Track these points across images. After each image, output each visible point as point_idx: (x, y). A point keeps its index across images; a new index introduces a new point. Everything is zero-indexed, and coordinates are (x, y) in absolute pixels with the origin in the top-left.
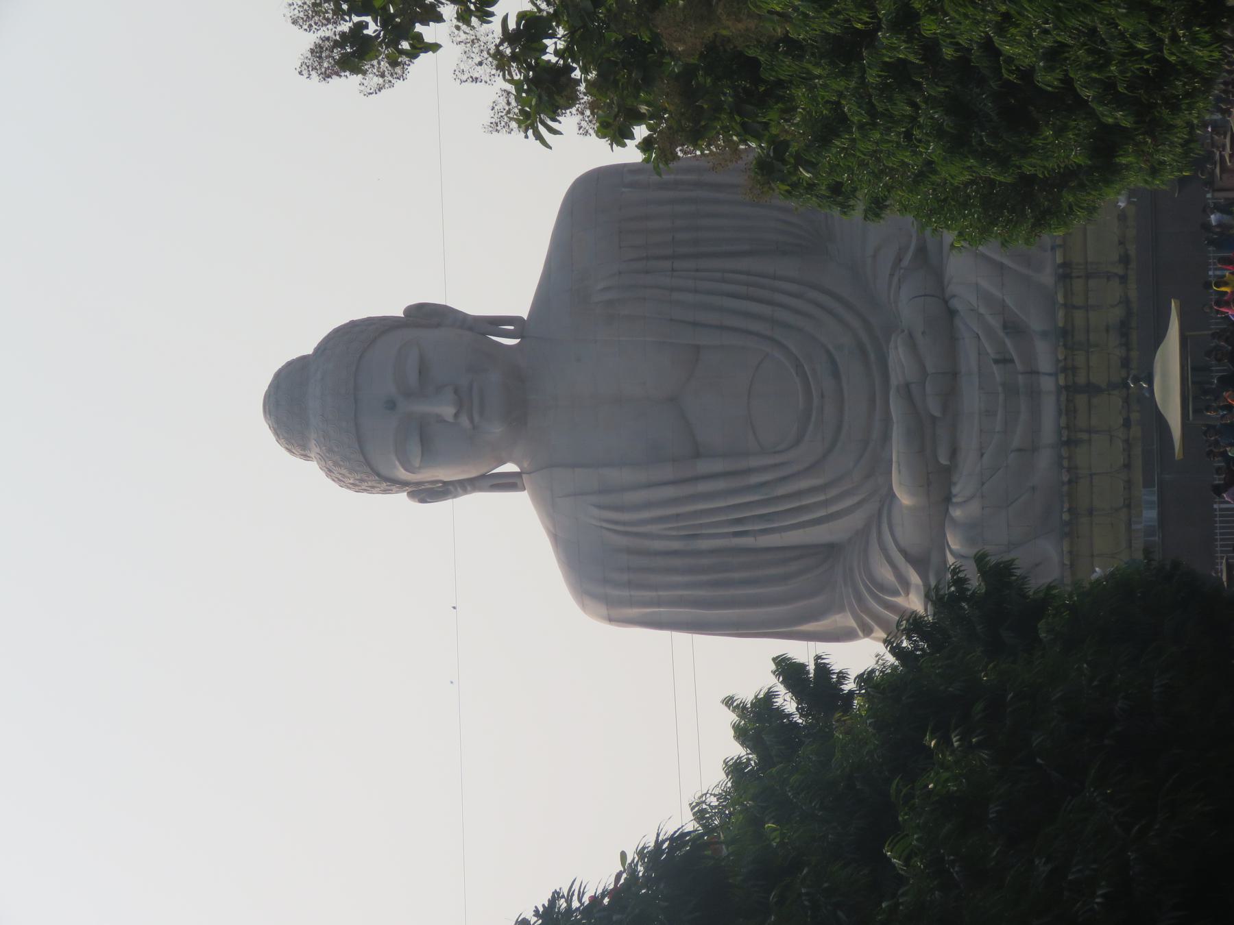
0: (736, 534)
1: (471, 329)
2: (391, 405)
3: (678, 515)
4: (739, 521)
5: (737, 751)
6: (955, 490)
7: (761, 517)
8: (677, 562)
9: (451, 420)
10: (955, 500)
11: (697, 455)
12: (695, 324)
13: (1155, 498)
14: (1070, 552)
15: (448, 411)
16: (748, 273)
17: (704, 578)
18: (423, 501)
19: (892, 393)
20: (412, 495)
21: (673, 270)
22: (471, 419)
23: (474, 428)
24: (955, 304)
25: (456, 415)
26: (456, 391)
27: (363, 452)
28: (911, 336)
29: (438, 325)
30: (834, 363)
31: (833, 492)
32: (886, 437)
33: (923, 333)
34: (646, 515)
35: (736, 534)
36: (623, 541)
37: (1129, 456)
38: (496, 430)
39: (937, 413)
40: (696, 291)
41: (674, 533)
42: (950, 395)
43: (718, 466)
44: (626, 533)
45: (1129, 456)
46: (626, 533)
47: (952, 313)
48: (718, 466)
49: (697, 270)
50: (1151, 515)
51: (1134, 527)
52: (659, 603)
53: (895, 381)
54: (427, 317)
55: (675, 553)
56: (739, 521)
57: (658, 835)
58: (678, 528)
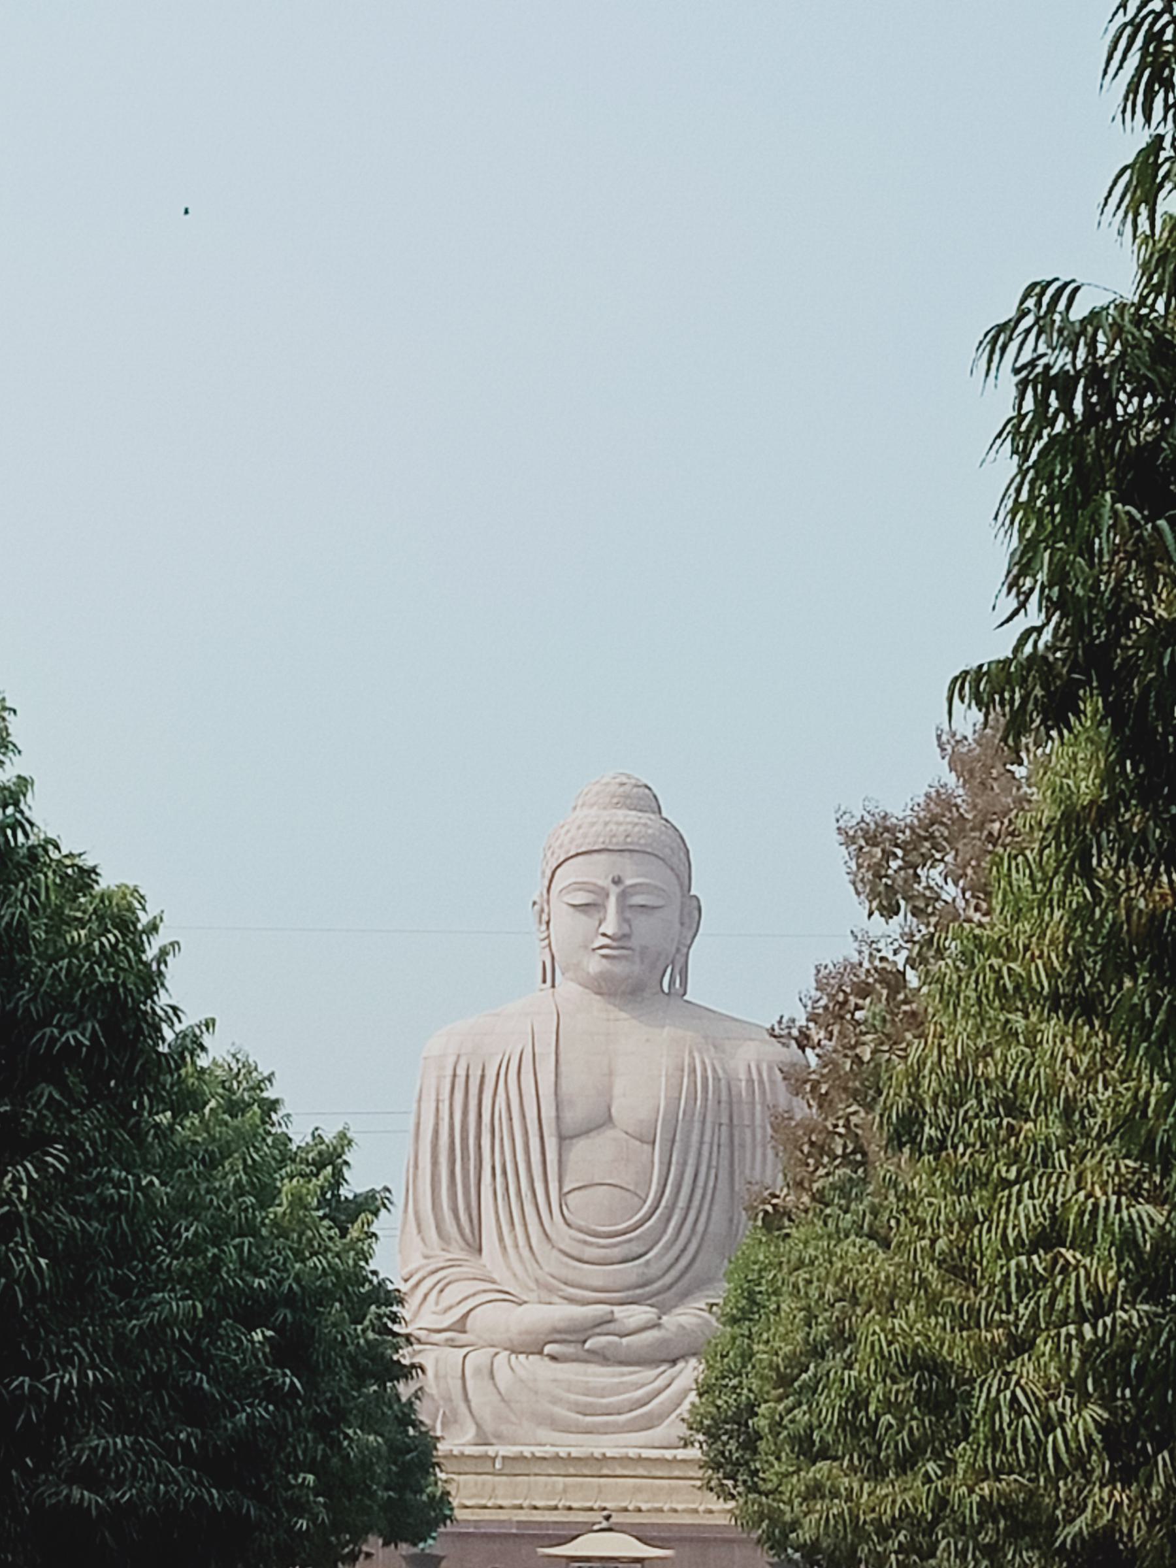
0: (493, 1168)
2: (617, 881)
4: (504, 1173)
5: (105, 883)
6: (522, 1357)
7: (507, 1189)
9: (602, 930)
10: (513, 1357)
11: (561, 1138)
12: (673, 1141)
14: (462, 1455)
15: (610, 927)
16: (715, 1187)
19: (607, 1308)
21: (720, 1125)
22: (601, 948)
23: (594, 950)
24: (681, 1365)
25: (604, 935)
26: (626, 936)
29: (682, 924)
31: (525, 1252)
32: (571, 1300)
35: (493, 1168)
39: (587, 1345)
40: (701, 1143)
42: (602, 1357)
43: (551, 1156)
47: (674, 1362)
48: (551, 1156)
49: (719, 1146)
53: (616, 1309)
54: (691, 913)
56: (504, 1173)
57: (167, 990)
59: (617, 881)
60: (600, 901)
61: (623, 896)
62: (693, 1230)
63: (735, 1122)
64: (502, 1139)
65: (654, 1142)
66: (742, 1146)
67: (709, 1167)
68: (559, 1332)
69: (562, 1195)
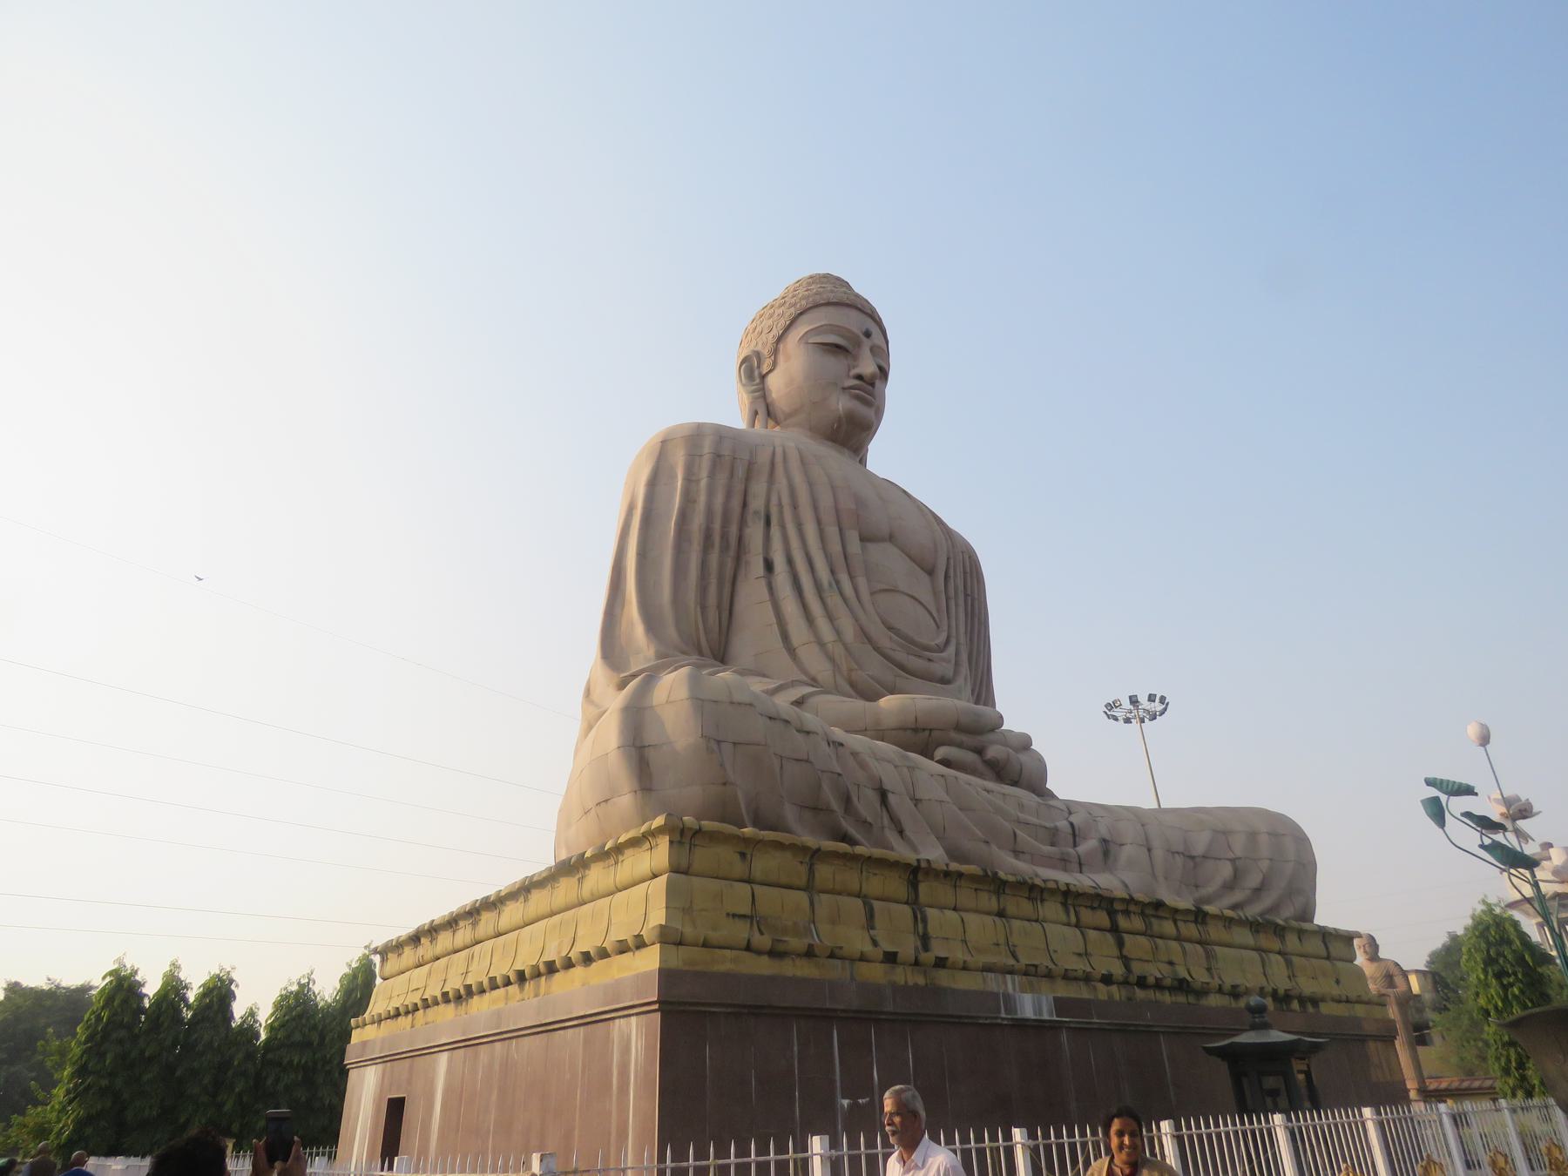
8: (736, 504)
13: (1046, 1017)
17: (717, 526)
22: (851, 388)
25: (859, 377)
27: (828, 304)
34: (798, 479)
36: (779, 451)
37: (1076, 979)
41: (774, 500)
44: (773, 464)
45: (1076, 979)
46: (773, 464)
50: (1030, 1005)
51: (1008, 977)
52: (690, 479)
55: (745, 505)
58: (780, 505)
60: (850, 347)
64: (783, 527)
68: (959, 727)
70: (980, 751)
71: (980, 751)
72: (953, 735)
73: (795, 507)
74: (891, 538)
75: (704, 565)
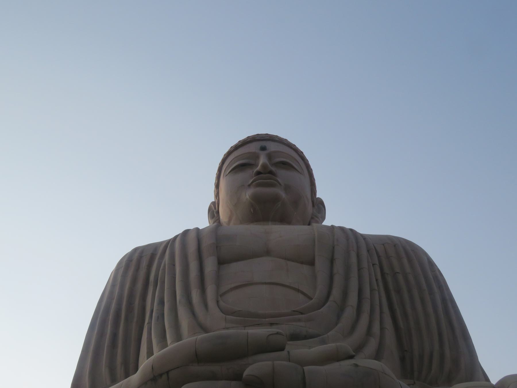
1: (312, 218)
3: (174, 265)
11: (221, 262)
12: (332, 261)
18: (210, 209)
20: (213, 203)
23: (249, 186)
25: (258, 173)
26: (271, 172)
28: (351, 357)
29: (313, 206)
30: (306, 337)
33: (356, 365)
38: (247, 195)
40: (360, 269)
58: (164, 269)
59: (263, 149)
61: (270, 157)
62: (369, 332)
63: (386, 270)
64: (163, 282)
65: (312, 263)
66: (399, 291)
67: (372, 290)
69: (220, 295)
70: (237, 377)
71: (237, 377)
72: (196, 368)
73: (173, 265)
74: (268, 253)
75: (115, 335)
